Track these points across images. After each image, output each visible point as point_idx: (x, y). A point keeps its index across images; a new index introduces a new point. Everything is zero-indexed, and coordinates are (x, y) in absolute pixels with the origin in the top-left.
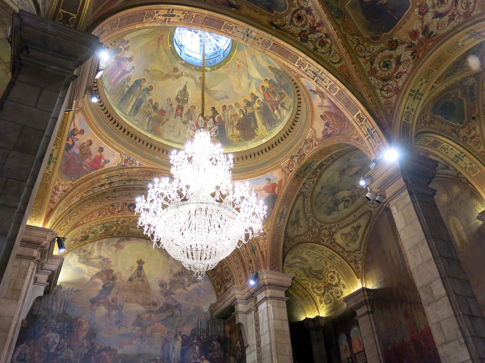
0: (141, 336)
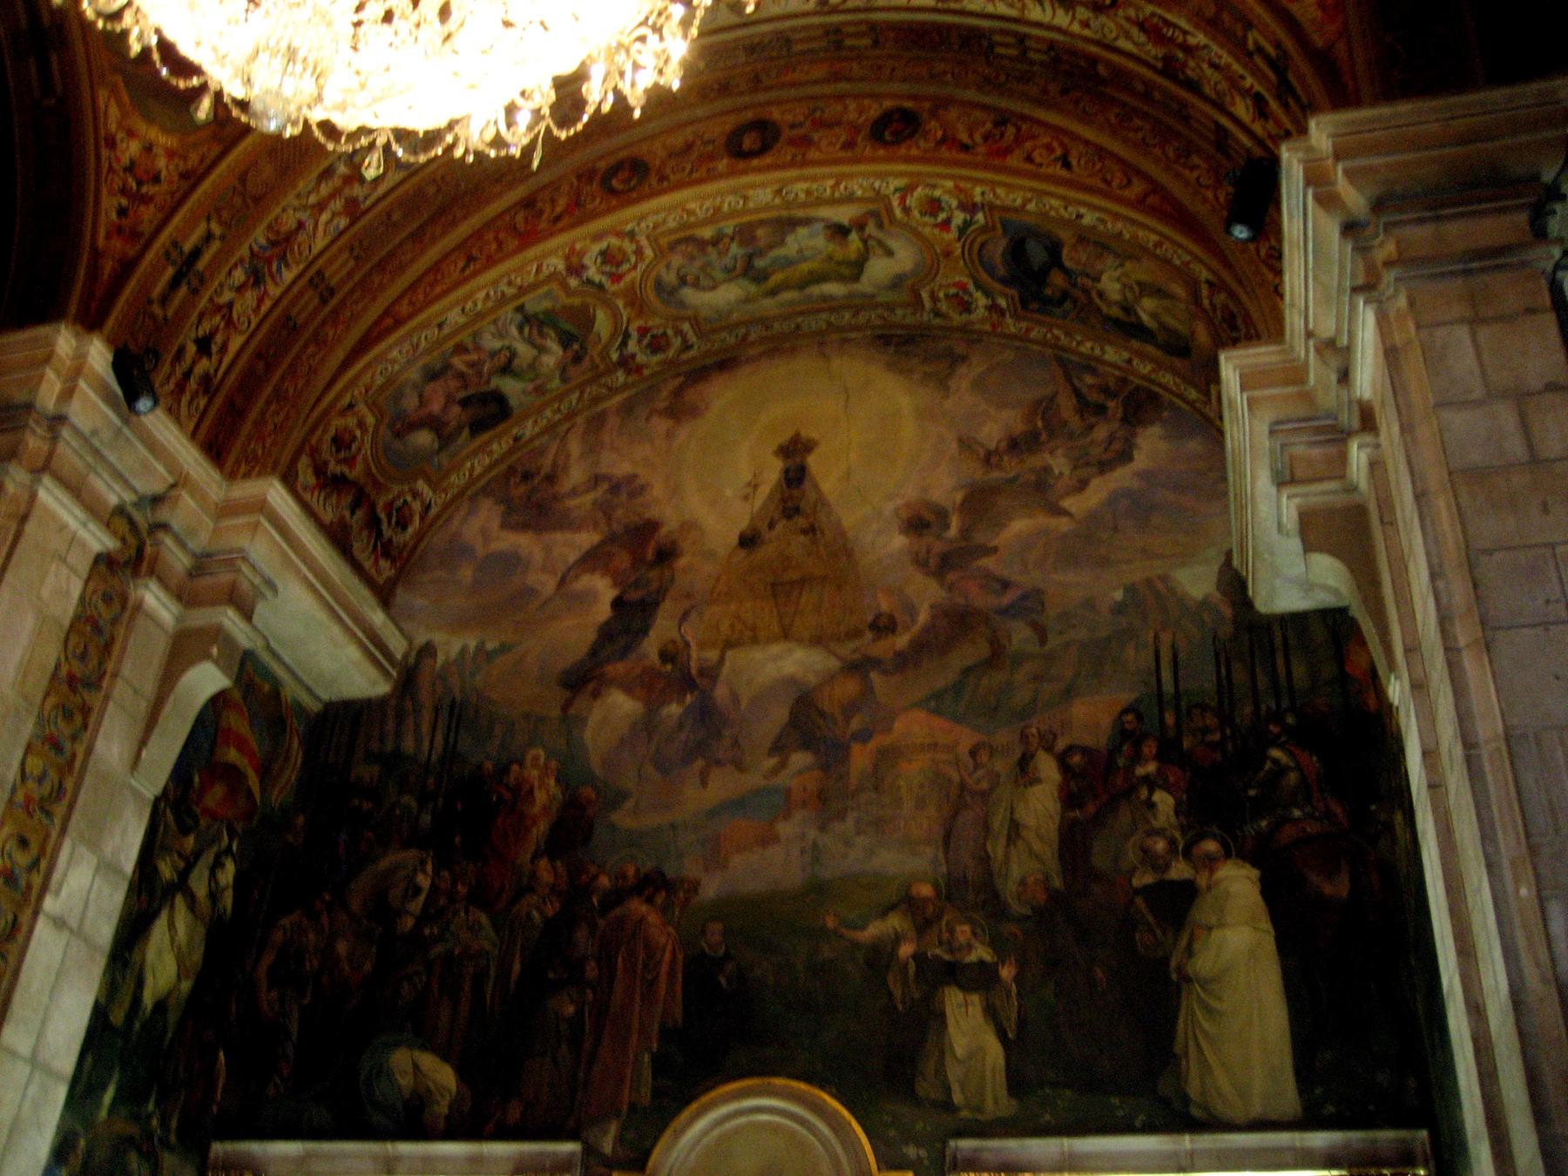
0: (822, 797)
